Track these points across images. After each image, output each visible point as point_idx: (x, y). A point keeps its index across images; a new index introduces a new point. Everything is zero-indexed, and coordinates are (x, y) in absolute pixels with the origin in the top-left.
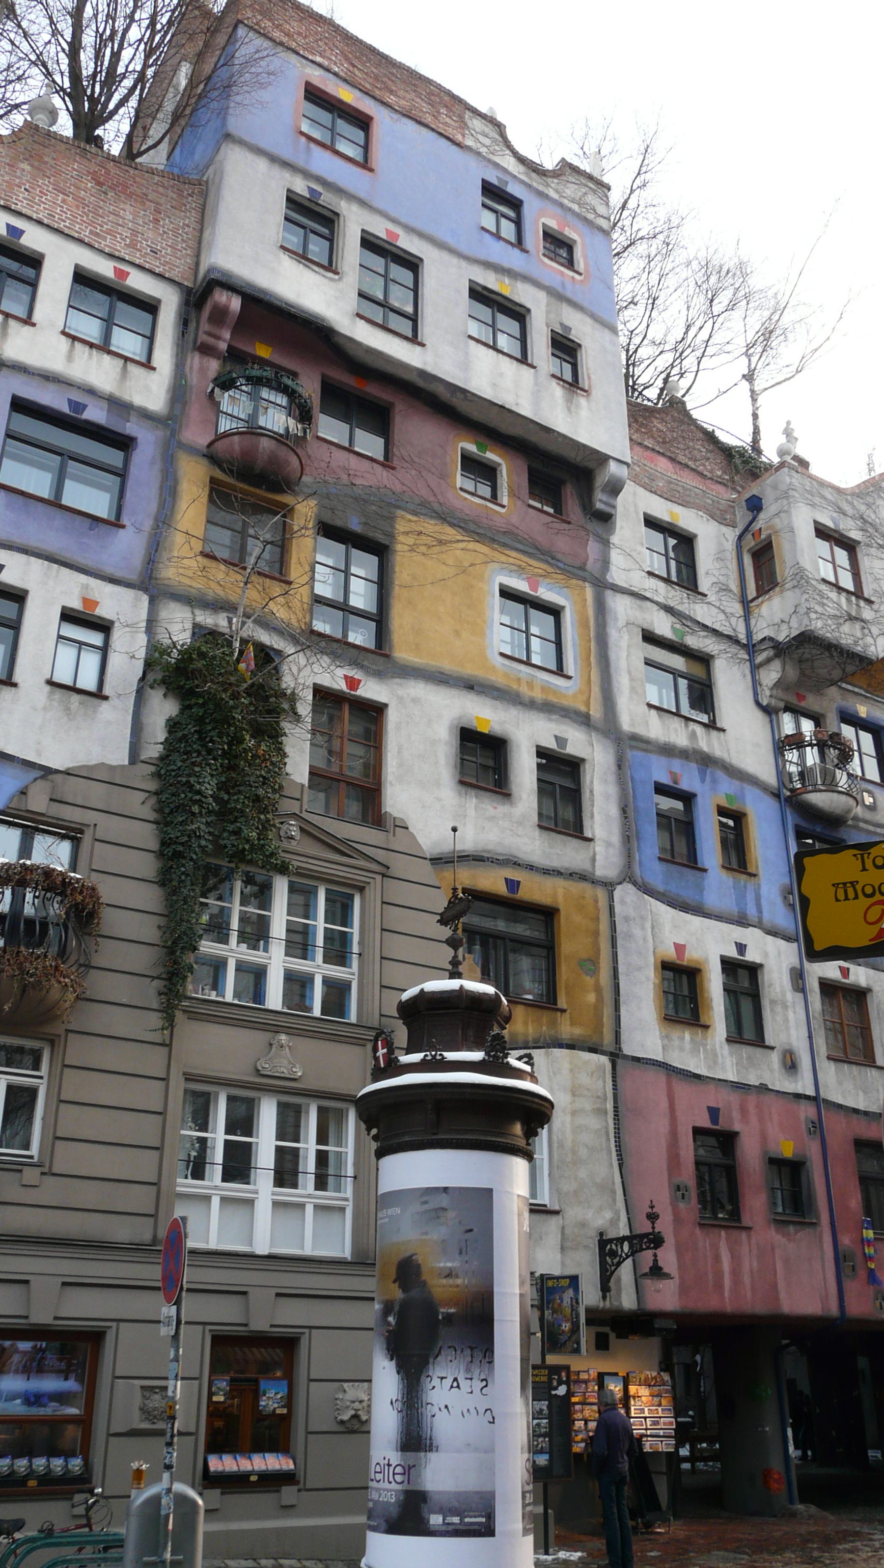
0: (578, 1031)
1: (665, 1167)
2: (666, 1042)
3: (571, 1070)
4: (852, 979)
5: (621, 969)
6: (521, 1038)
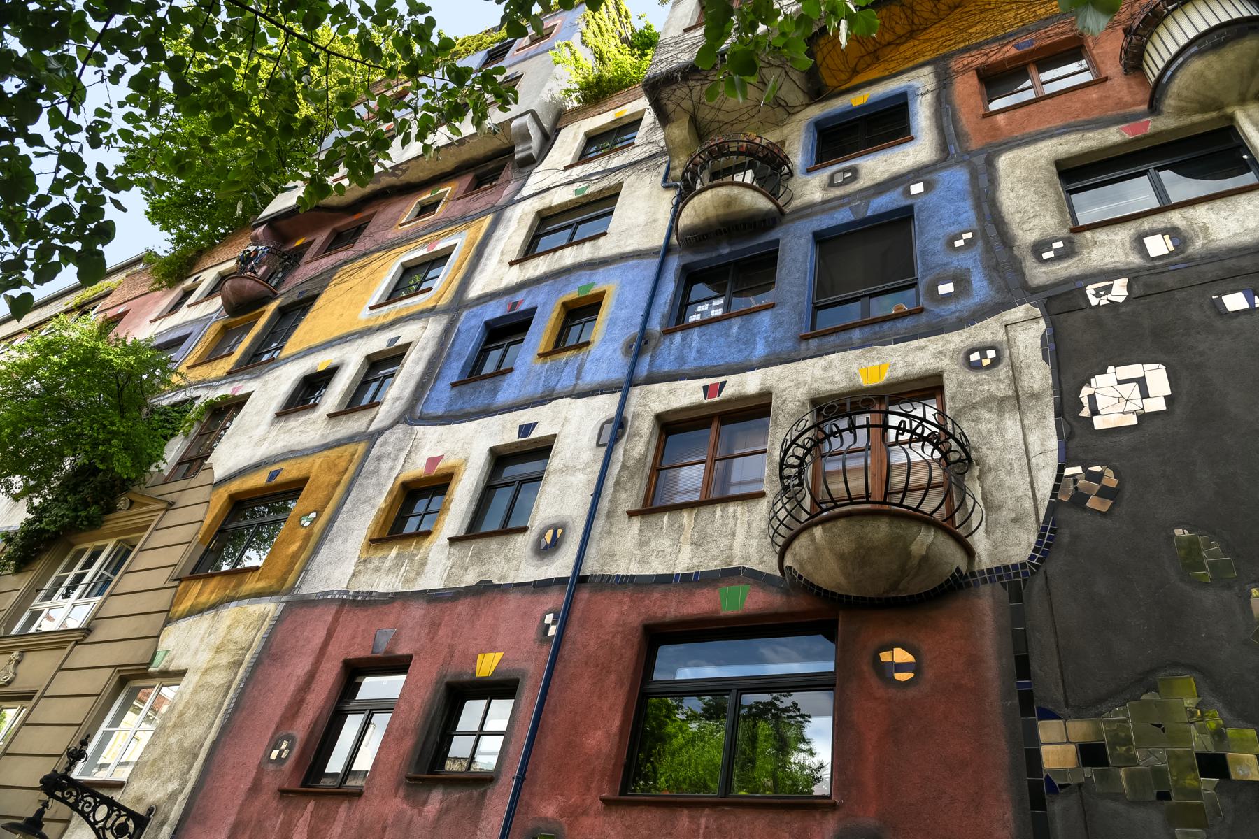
0: (261, 584)
1: (277, 719)
2: (361, 567)
3: (229, 627)
4: (727, 392)
5: (348, 505)
6: (201, 606)
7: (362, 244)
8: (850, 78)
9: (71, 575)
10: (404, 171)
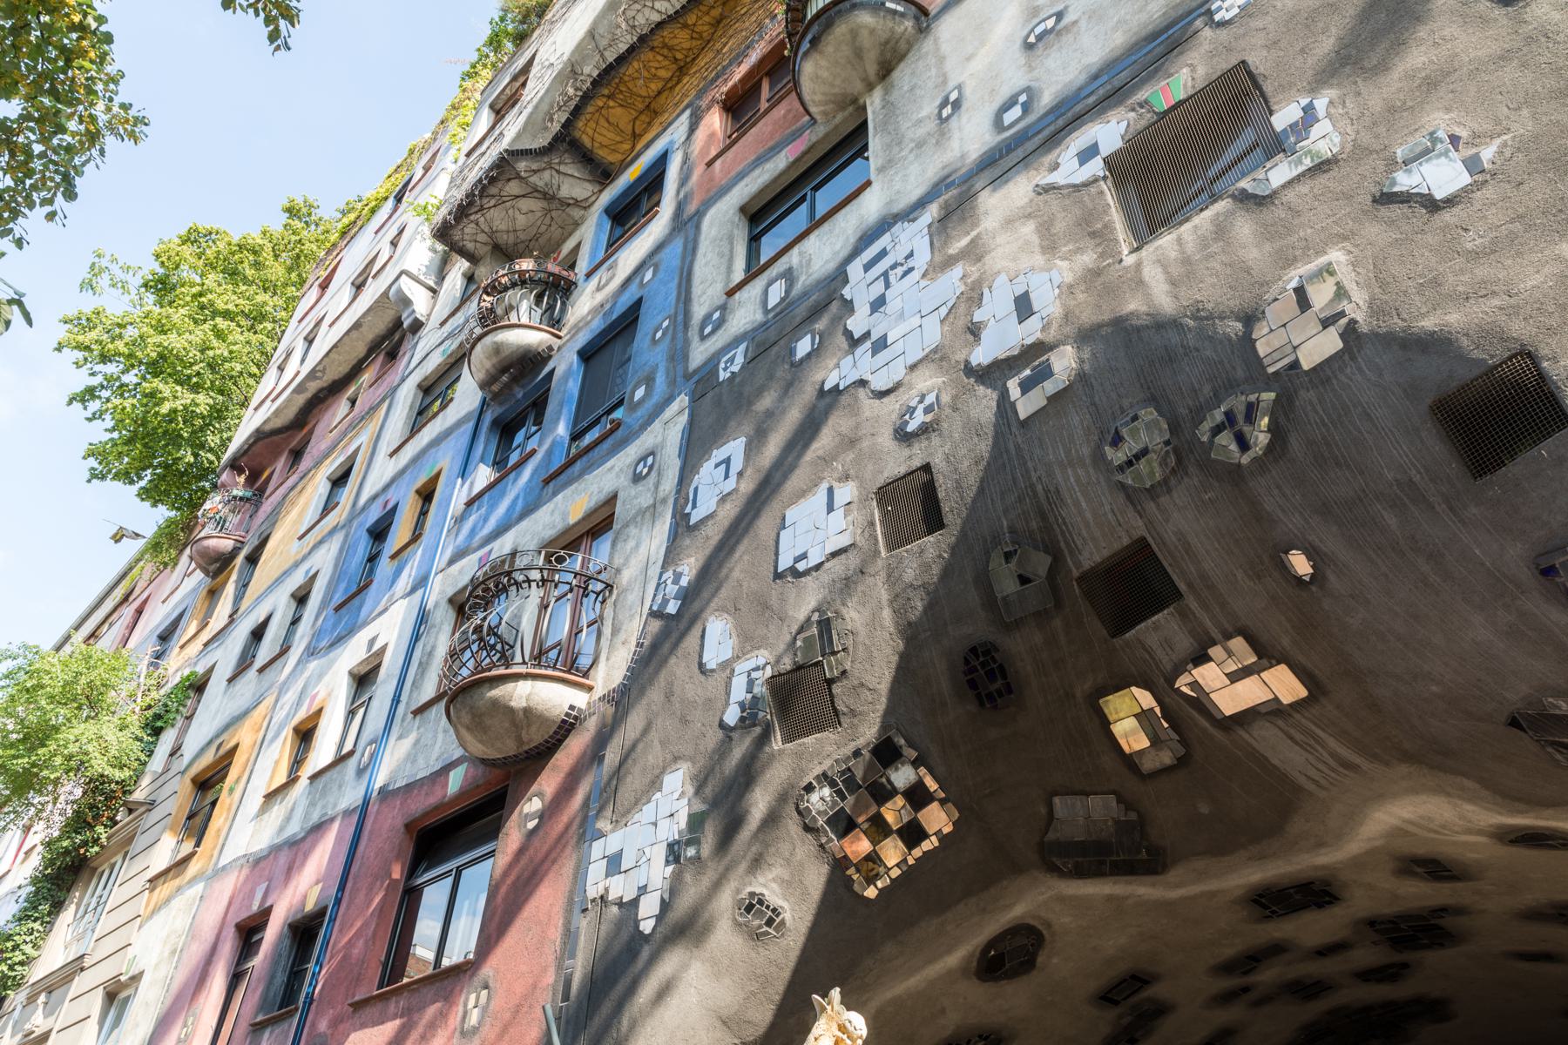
7: (306, 462)
8: (634, 147)
9: (94, 900)
10: (323, 371)
